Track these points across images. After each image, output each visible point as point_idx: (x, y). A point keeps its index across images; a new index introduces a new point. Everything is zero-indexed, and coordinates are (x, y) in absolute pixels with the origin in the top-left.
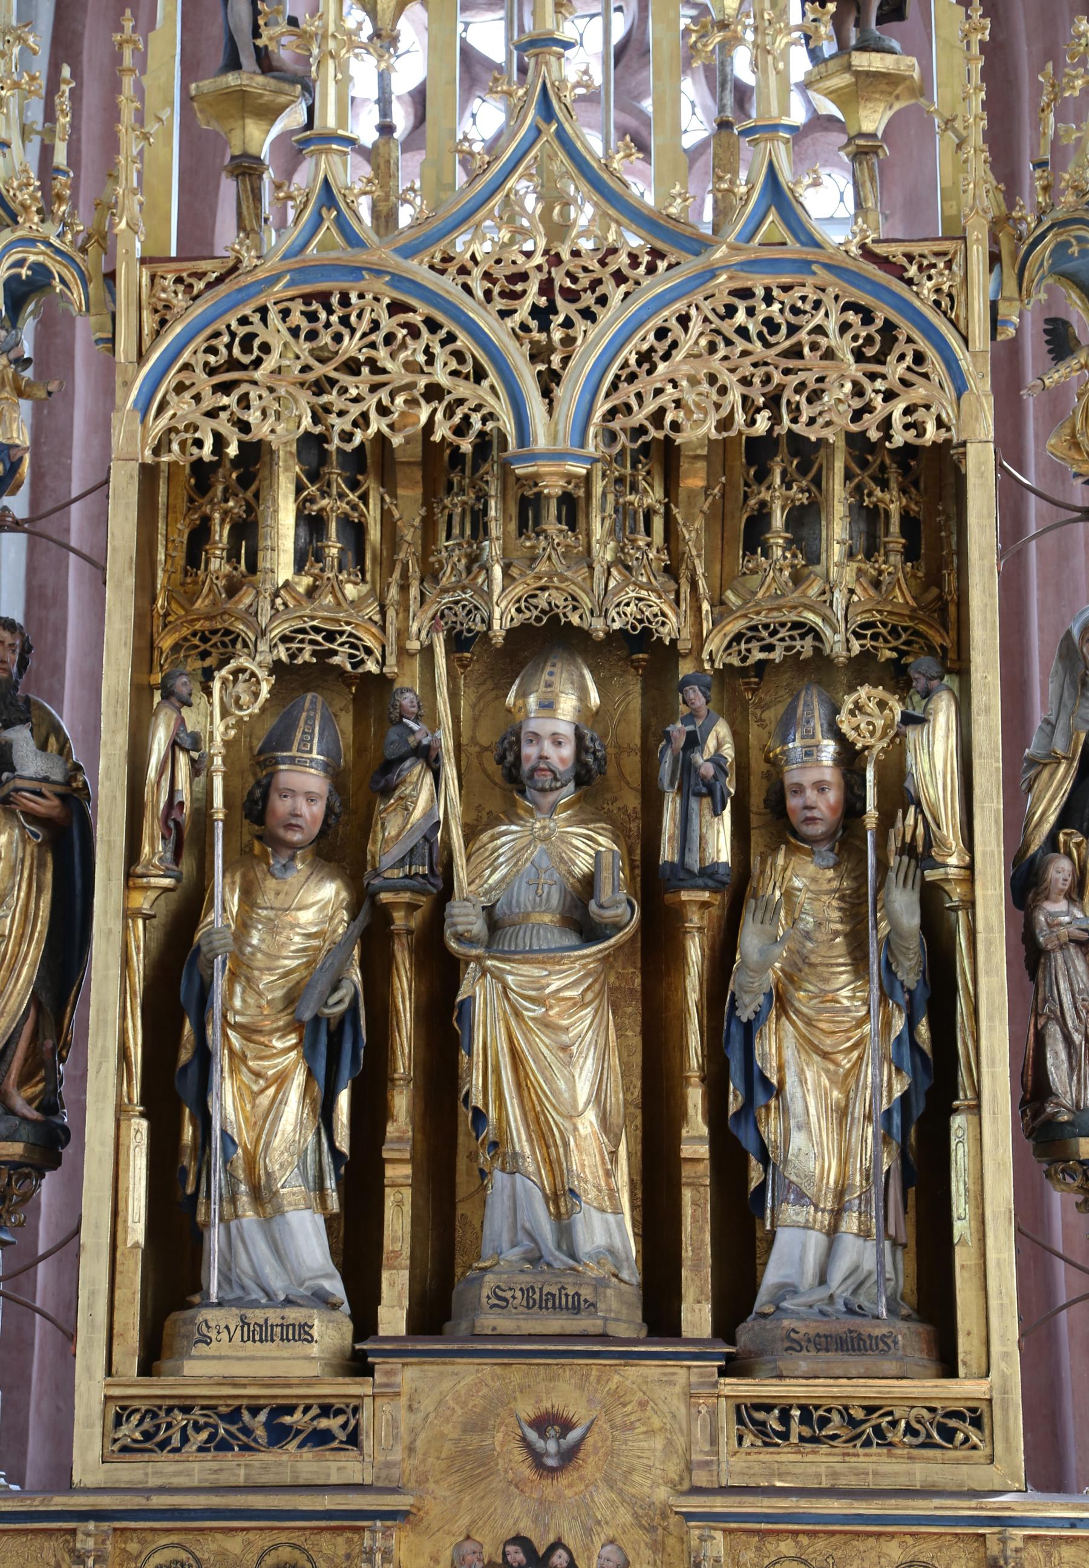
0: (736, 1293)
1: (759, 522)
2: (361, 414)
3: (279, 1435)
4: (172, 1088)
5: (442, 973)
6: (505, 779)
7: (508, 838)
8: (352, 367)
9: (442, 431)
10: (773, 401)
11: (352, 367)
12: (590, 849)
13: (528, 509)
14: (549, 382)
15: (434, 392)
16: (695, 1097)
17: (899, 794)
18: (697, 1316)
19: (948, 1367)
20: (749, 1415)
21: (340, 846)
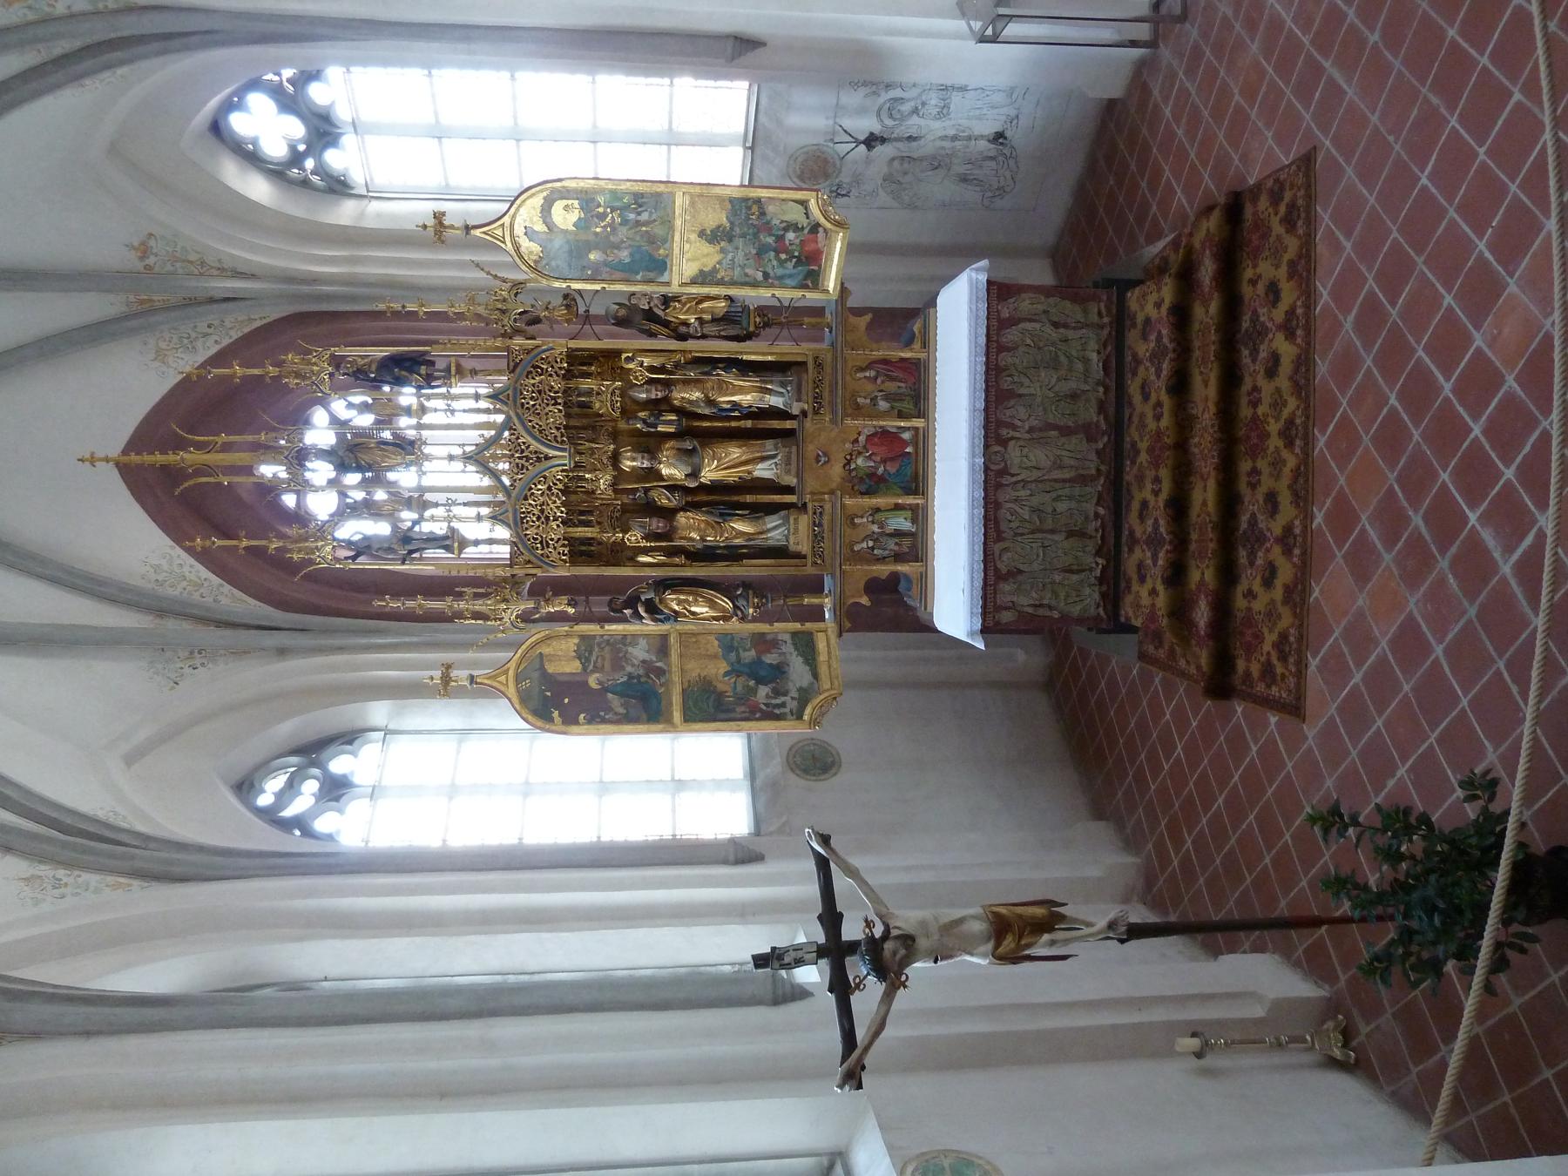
0: (782, 414)
1: (583, 405)
2: (557, 509)
3: (820, 525)
4: (733, 554)
5: (703, 488)
6: (653, 474)
7: (665, 471)
8: (542, 511)
9: (560, 486)
10: (554, 398)
11: (542, 511)
12: (667, 453)
13: (578, 466)
14: (547, 458)
15: (549, 488)
16: (733, 424)
17: (662, 369)
18: (788, 424)
19: (804, 364)
20: (816, 412)
21: (668, 514)
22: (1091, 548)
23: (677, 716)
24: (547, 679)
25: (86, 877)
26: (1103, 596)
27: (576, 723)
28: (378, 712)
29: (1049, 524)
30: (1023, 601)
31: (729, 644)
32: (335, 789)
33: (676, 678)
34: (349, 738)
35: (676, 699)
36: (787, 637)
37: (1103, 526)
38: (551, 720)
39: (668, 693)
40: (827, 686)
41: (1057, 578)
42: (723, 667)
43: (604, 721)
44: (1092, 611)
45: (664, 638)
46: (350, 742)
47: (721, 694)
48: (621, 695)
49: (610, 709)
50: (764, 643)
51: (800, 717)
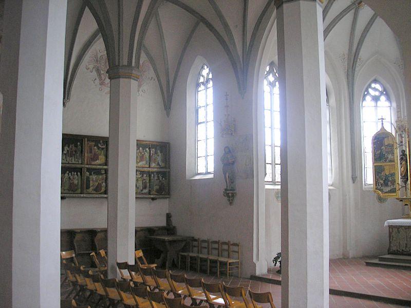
22: (404, 249)
23: (376, 164)
24: (384, 138)
25: (346, 63)
26: (394, 251)
27: (374, 145)
28: (394, 104)
29: (408, 240)
30: (393, 234)
31: (393, 175)
32: (376, 99)
33: (384, 164)
34: (389, 99)
35: (379, 164)
36: (395, 187)
37: (408, 252)
38: (374, 140)
39: (381, 163)
40: (384, 195)
41: (398, 241)
42: (387, 174)
43: (374, 150)
44: (391, 248)
45: (394, 161)
46: (388, 99)
47: (381, 173)
48: (380, 153)
49: (377, 151)
50: (393, 182)
51: (376, 189)
